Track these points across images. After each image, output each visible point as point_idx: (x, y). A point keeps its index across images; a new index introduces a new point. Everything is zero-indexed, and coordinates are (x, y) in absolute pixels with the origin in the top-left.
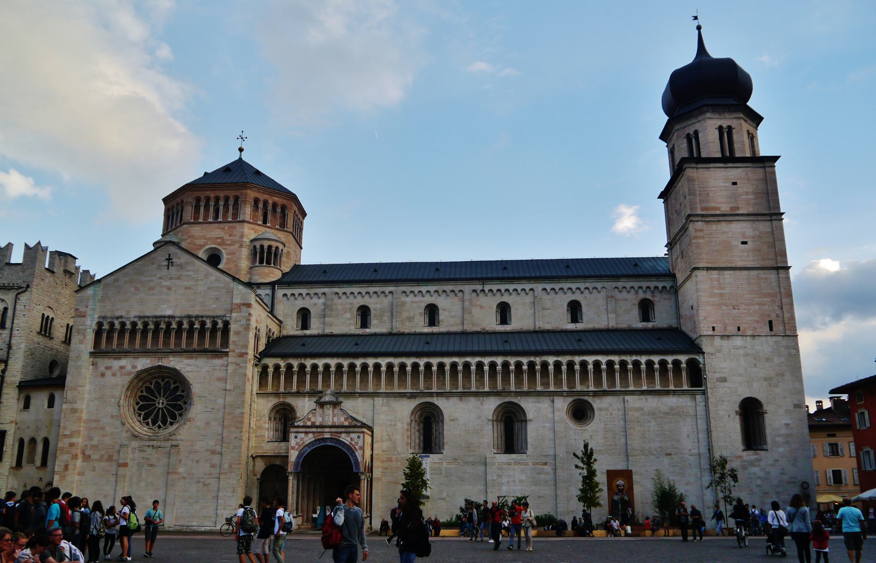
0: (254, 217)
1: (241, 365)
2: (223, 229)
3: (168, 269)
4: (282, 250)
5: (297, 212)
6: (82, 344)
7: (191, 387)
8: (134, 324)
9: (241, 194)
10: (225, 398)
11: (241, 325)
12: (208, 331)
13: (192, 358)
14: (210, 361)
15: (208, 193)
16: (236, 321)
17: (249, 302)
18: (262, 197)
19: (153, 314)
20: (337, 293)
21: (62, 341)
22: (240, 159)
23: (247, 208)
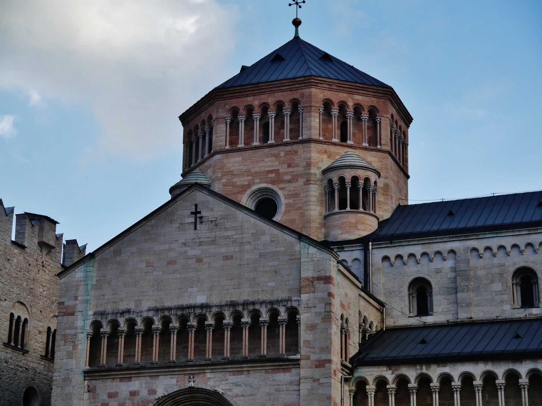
0: (326, 131)
1: (322, 381)
2: (277, 156)
3: (195, 229)
4: (375, 183)
5: (396, 117)
6: (72, 358)
8: (149, 322)
9: (302, 95)
11: (318, 314)
12: (264, 326)
13: (241, 372)
14: (270, 376)
15: (250, 99)
16: (308, 307)
17: (327, 275)
18: (336, 97)
19: (176, 304)
20: (475, 249)
21: (41, 356)
22: (297, 38)
23: (312, 119)
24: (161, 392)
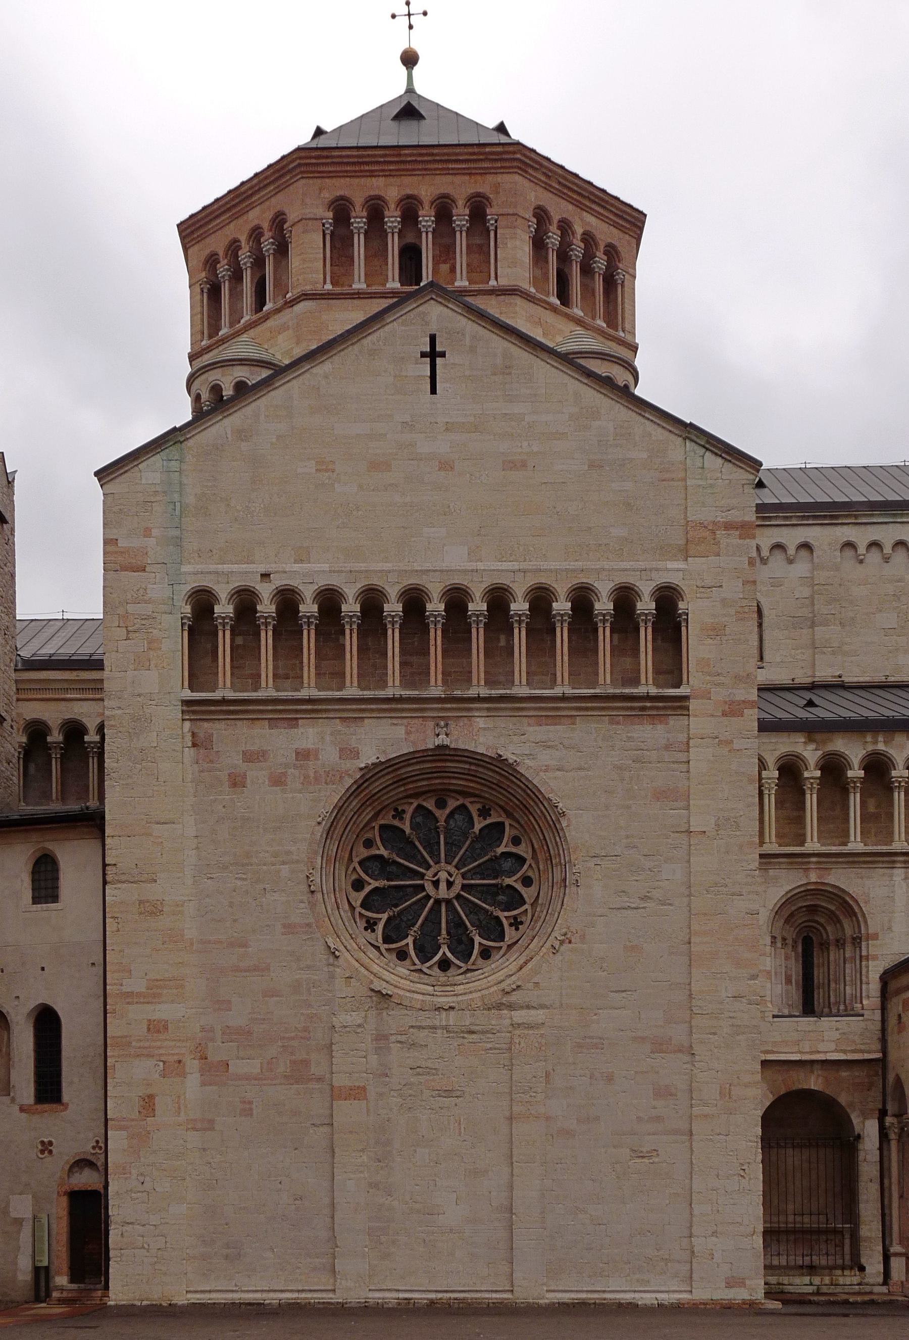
7: (564, 824)
10: (689, 861)
22: (410, 90)
24: (369, 756)
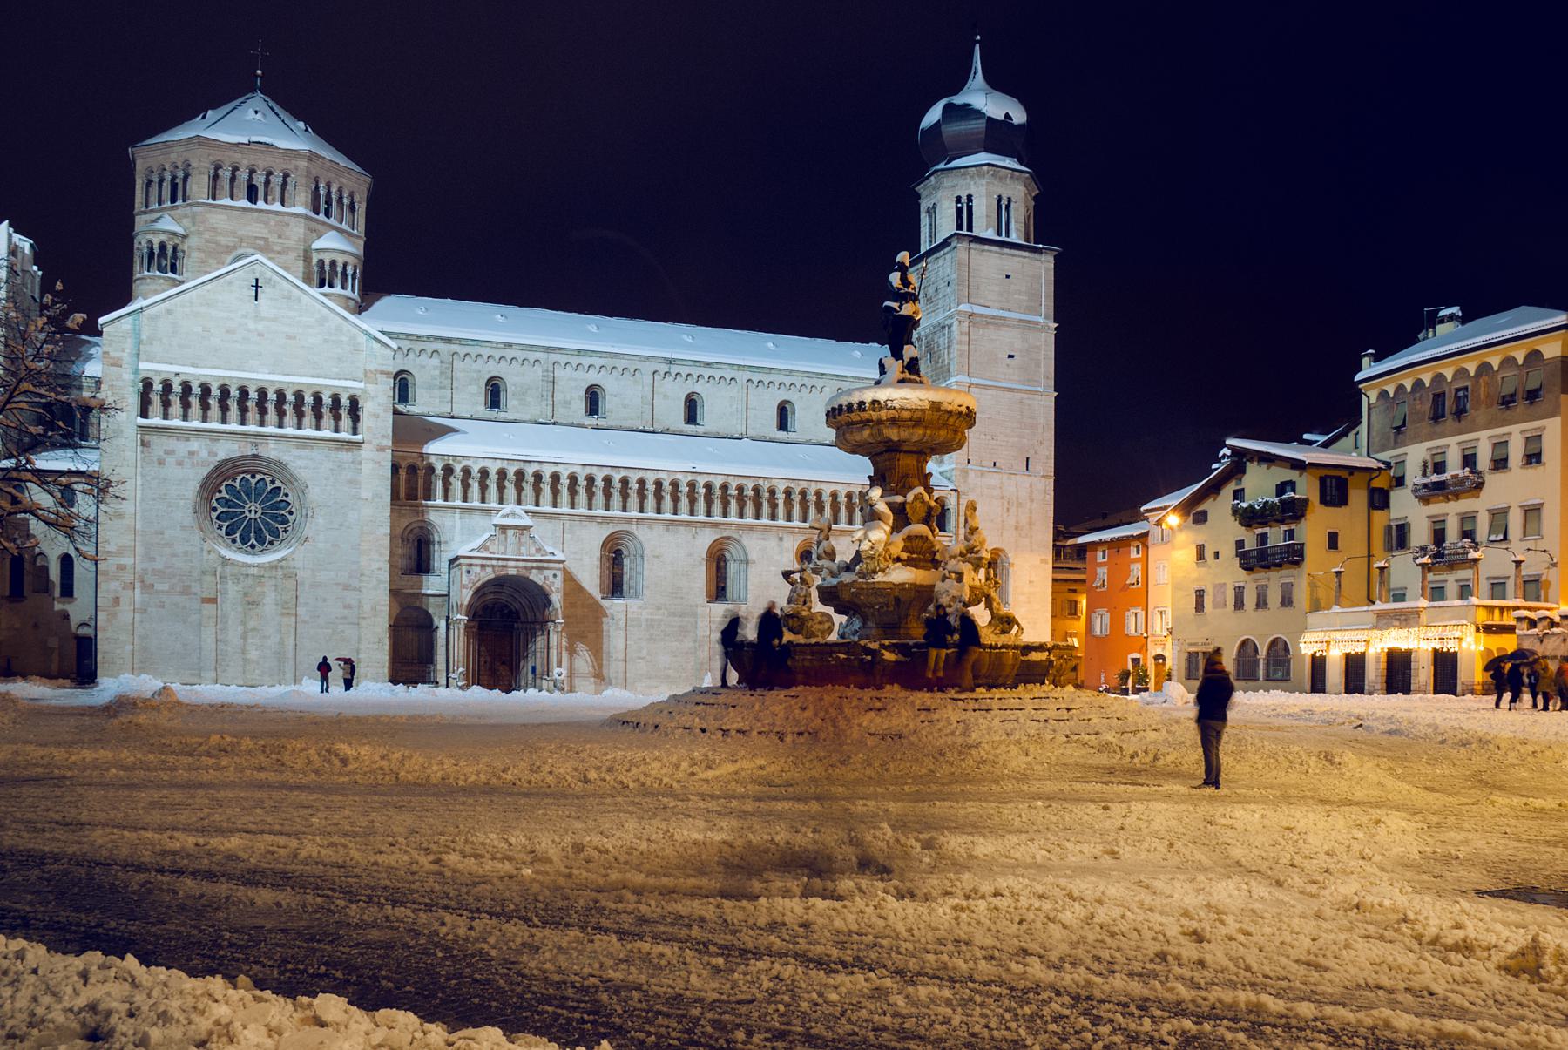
2: (266, 223)
9: (296, 168)
11: (379, 404)
13: (304, 447)
14: (333, 454)
24: (222, 456)
